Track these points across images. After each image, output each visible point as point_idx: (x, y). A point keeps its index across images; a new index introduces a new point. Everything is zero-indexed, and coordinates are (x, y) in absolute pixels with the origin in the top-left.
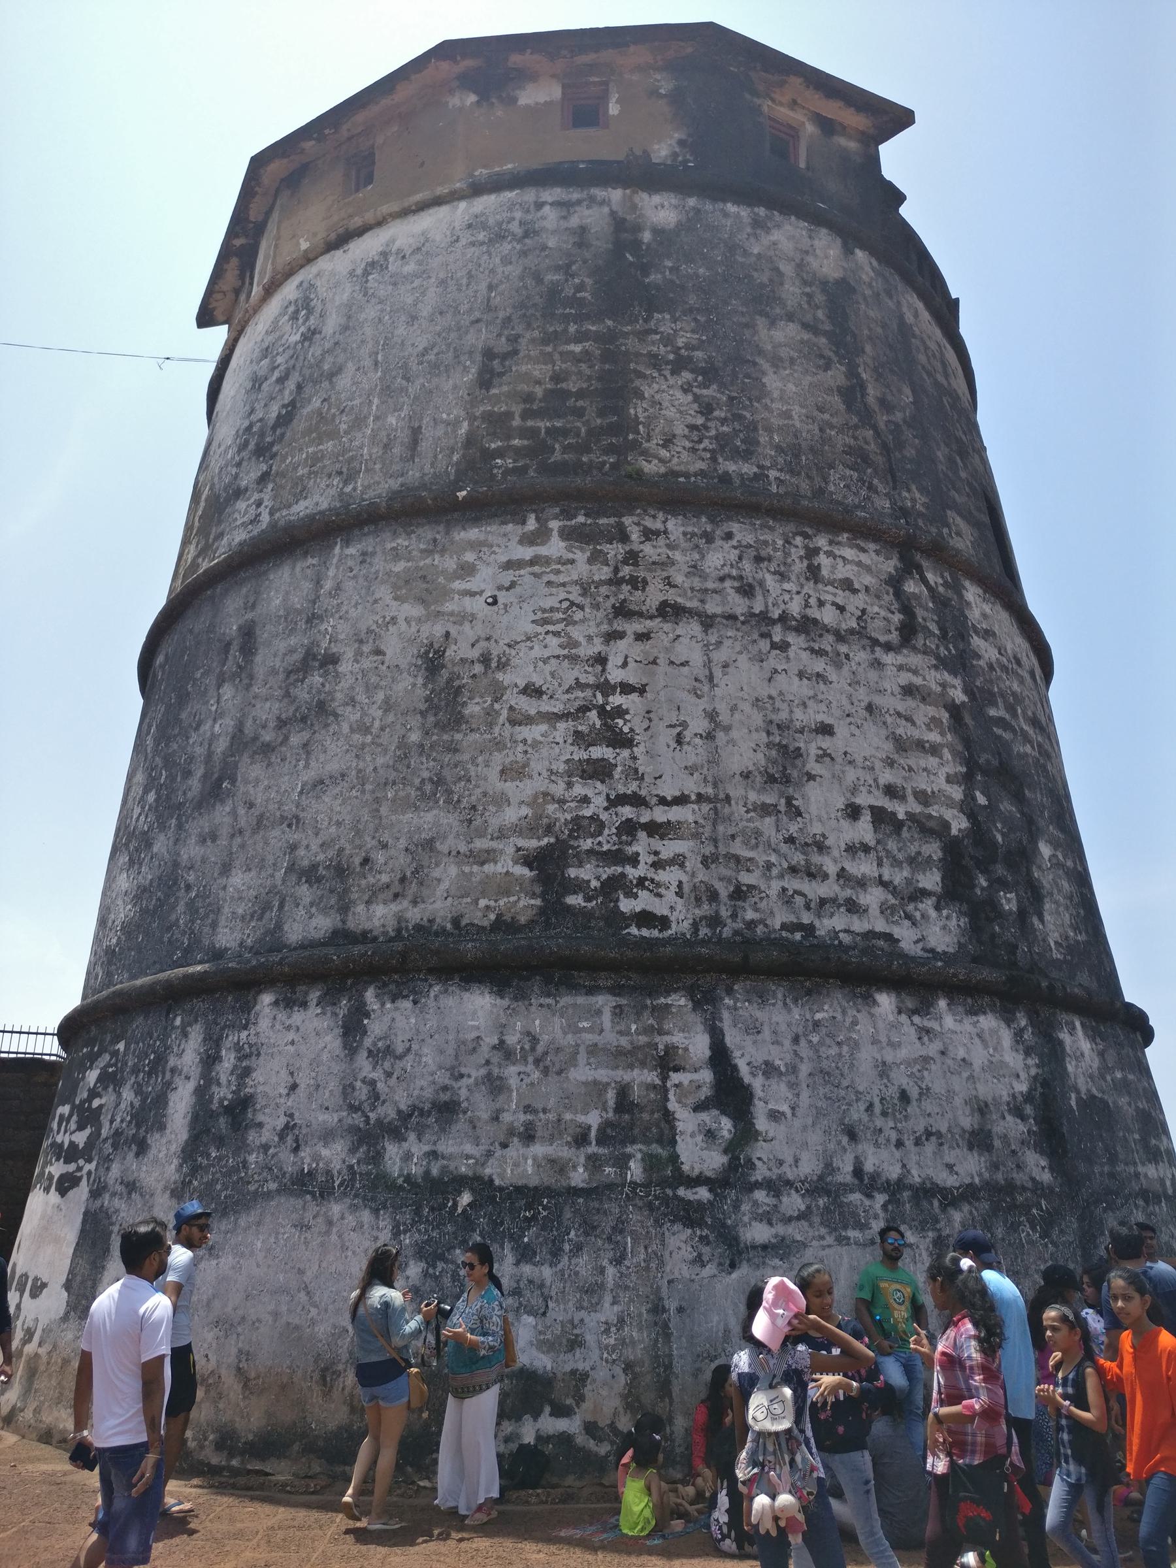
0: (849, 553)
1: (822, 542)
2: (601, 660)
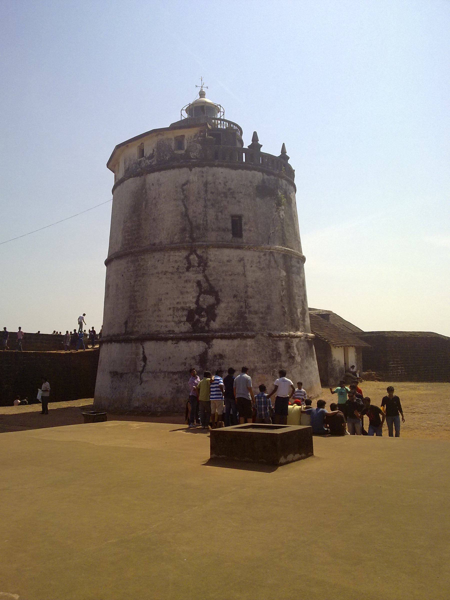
0: (177, 254)
1: (172, 253)
2: (134, 286)
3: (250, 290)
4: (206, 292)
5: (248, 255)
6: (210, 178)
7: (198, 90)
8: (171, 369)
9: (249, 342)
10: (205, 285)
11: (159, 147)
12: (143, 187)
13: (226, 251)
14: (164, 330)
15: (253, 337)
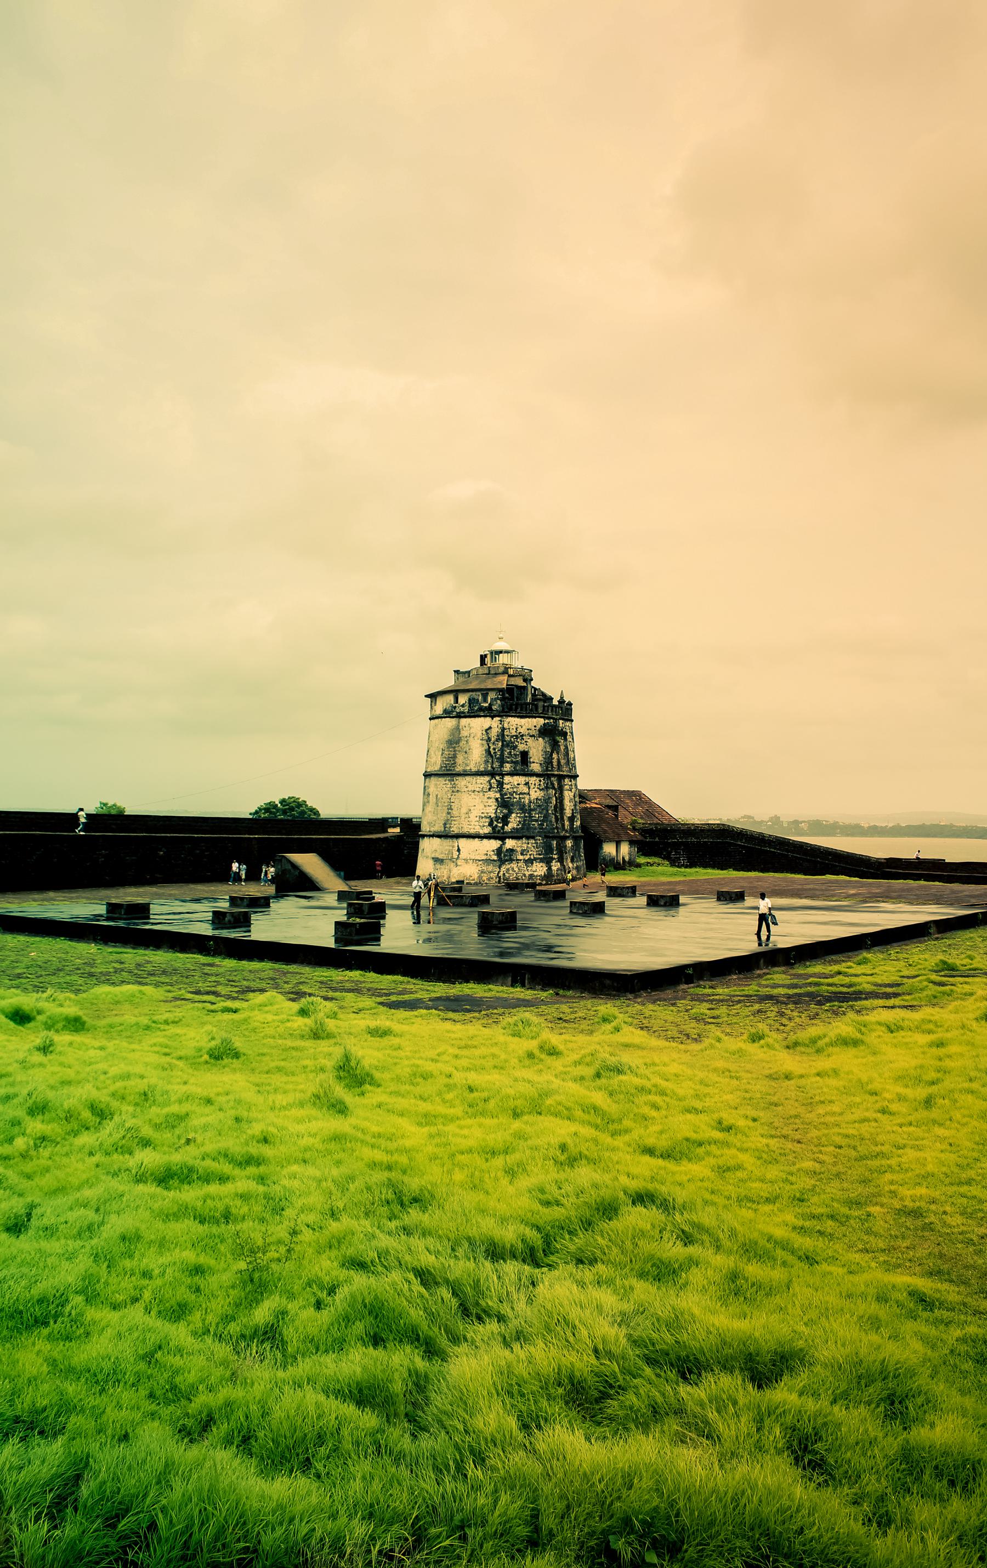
5: (533, 780)
6: (506, 726)
12: (458, 729)
13: (516, 778)
14: (472, 831)
15: (533, 838)
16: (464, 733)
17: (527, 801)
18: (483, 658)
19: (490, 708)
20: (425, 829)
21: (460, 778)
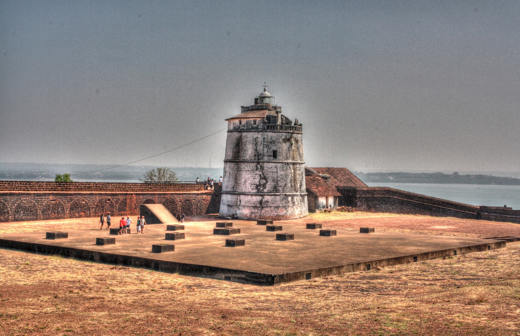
3: (279, 179)
4: (262, 179)
5: (279, 165)
6: (266, 137)
7: (264, 87)
8: (250, 205)
9: (277, 197)
10: (262, 176)
11: (247, 123)
13: (271, 164)
14: (247, 191)
15: (279, 195)
16: (244, 140)
17: (276, 176)
18: (256, 100)
19: (257, 128)
20: (224, 189)
21: (241, 164)
